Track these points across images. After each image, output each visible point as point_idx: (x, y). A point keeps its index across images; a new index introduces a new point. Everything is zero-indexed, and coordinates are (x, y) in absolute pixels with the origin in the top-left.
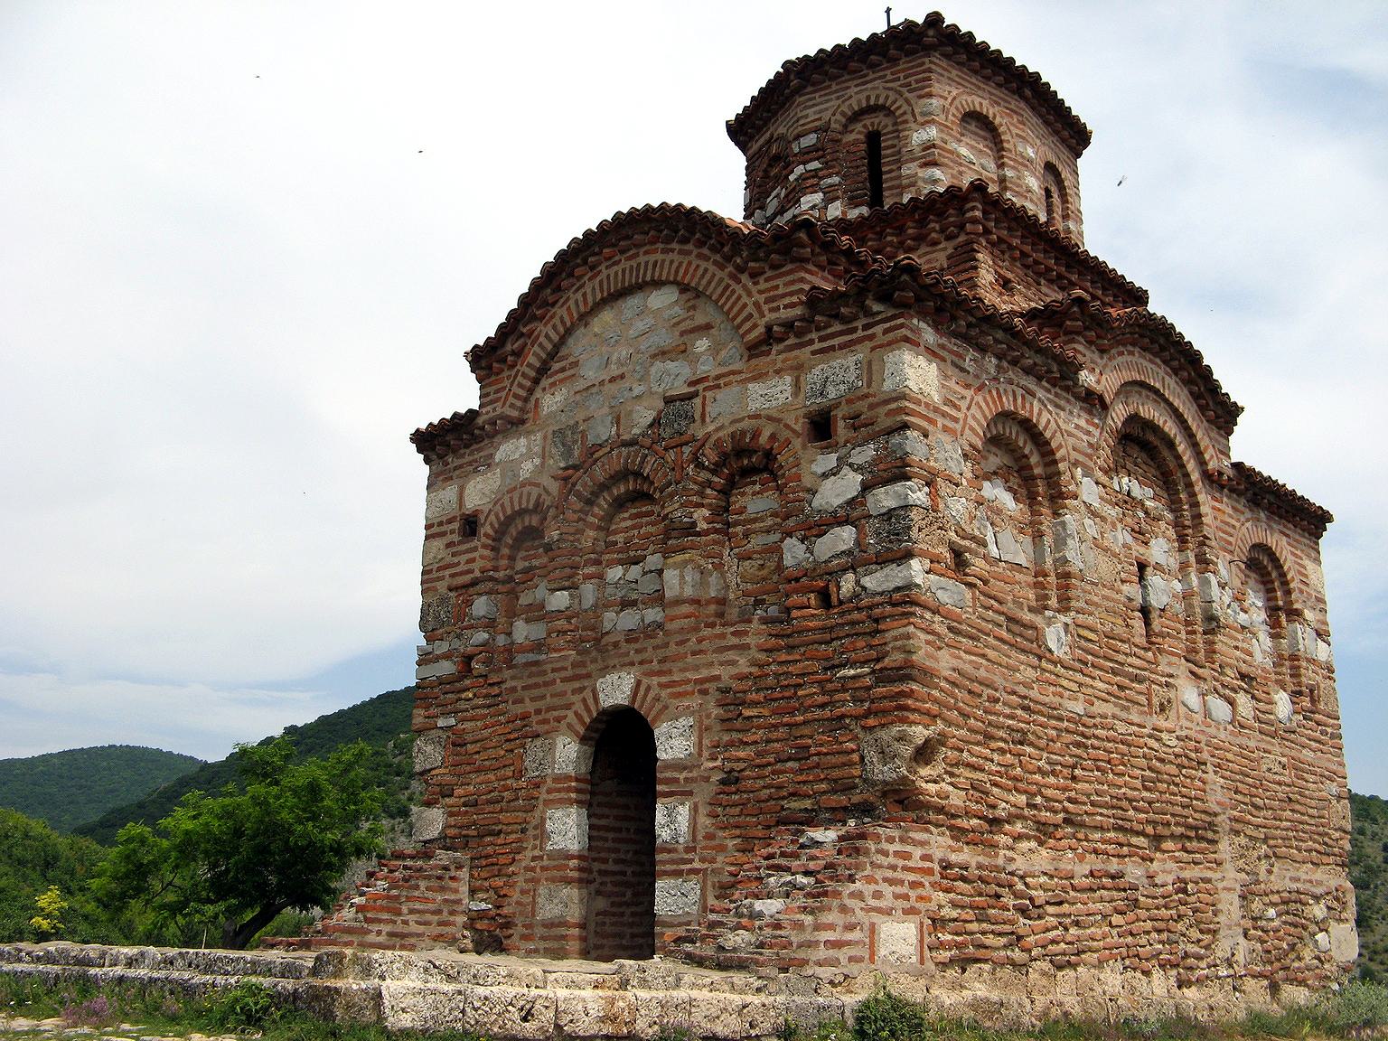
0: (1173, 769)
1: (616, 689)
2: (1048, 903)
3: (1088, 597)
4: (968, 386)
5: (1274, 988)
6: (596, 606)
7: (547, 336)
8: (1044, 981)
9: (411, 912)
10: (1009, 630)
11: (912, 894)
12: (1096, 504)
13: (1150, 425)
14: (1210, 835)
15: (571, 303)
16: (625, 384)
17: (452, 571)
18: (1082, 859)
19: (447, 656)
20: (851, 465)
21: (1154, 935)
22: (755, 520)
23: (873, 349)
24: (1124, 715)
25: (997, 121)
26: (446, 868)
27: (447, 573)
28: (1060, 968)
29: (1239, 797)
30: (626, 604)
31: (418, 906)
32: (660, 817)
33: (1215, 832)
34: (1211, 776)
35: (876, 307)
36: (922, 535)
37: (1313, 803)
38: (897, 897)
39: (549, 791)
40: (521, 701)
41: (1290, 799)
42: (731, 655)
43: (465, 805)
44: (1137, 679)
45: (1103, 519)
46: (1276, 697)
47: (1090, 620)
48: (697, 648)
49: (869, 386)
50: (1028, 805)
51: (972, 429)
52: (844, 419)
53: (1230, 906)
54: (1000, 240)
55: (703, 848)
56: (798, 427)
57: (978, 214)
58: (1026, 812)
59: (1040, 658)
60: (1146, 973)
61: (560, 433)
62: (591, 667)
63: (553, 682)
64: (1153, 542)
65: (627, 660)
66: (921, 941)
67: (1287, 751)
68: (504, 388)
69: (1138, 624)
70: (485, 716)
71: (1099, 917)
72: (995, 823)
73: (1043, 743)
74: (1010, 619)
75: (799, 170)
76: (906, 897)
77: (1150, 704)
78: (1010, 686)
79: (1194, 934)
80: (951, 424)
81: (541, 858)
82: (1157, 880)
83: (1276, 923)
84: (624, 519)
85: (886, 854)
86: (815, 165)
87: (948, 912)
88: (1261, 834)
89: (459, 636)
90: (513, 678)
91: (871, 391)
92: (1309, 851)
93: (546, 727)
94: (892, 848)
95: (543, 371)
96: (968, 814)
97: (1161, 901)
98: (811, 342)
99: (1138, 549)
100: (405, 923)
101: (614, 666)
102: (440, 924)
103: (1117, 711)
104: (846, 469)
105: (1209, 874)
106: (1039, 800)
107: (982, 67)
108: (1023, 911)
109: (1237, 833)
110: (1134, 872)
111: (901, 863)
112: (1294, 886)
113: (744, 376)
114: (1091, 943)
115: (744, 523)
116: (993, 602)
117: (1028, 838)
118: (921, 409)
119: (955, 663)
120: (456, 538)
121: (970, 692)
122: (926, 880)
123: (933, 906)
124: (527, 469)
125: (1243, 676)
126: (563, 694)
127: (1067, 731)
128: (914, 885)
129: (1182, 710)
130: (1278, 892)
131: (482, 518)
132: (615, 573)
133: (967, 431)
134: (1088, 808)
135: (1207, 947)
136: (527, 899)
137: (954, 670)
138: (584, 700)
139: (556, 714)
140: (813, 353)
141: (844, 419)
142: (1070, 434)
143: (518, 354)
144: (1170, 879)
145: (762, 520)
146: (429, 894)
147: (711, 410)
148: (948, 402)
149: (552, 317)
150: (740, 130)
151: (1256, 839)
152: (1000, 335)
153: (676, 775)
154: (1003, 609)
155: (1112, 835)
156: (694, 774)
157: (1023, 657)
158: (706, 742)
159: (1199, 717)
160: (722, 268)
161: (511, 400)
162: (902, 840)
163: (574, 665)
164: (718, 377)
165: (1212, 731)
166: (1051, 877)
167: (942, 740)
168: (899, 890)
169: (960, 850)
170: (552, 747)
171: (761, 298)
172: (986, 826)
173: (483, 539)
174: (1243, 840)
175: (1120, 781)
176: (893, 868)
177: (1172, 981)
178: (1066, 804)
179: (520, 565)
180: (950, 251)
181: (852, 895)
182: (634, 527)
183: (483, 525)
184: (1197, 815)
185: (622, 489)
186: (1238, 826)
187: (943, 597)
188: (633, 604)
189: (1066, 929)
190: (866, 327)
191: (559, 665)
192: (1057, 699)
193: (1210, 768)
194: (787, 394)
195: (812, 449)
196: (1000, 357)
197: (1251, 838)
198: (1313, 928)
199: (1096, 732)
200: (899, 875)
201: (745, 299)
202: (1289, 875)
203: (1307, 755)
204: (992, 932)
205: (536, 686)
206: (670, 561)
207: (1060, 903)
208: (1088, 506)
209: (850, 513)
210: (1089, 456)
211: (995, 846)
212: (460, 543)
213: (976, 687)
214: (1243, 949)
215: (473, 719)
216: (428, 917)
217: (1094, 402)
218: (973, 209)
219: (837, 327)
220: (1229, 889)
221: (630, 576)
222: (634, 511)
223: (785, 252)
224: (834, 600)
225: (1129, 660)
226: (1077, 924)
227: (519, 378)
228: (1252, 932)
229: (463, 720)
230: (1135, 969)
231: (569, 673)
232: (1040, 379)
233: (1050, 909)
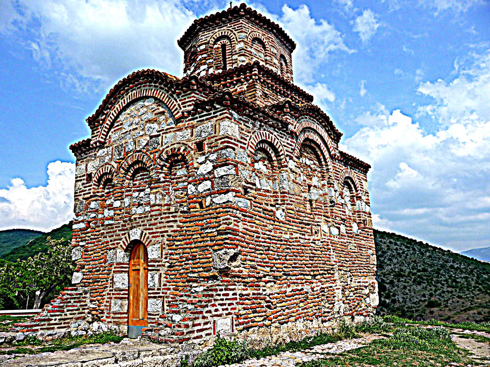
0: (319, 252)
1: (135, 234)
2: (277, 303)
4: (249, 132)
6: (129, 205)
7: (113, 114)
8: (277, 330)
9: (68, 311)
10: (264, 213)
11: (229, 308)
12: (294, 168)
13: (312, 141)
14: (332, 272)
15: (120, 103)
16: (137, 131)
17: (84, 193)
18: (289, 286)
19: (82, 221)
20: (209, 160)
21: (314, 308)
22: (179, 178)
24: (303, 237)
25: (264, 41)
26: (81, 294)
27: (82, 193)
28: (282, 324)
29: (341, 258)
30: (140, 205)
31: (70, 308)
34: (332, 253)
35: (217, 106)
36: (233, 184)
37: (365, 257)
38: (223, 310)
39: (115, 268)
42: (171, 224)
43: (88, 272)
44: (308, 224)
45: (296, 173)
46: (352, 225)
48: (161, 221)
49: (215, 133)
50: (271, 271)
51: (251, 147)
52: (207, 144)
53: (339, 293)
54: (264, 81)
55: (163, 289)
56: (193, 147)
57: (257, 72)
59: (274, 221)
60: (312, 321)
63: (116, 231)
64: (313, 178)
66: (233, 324)
67: (356, 242)
68: (99, 132)
69: (308, 205)
71: (295, 305)
73: (275, 249)
75: (200, 57)
76: (227, 309)
77: (312, 232)
79: (327, 305)
80: (244, 146)
82: (315, 289)
83: (354, 297)
84: (139, 176)
85: (219, 295)
86: (205, 55)
88: (348, 269)
89: (86, 215)
90: (103, 229)
91: (216, 135)
92: (363, 272)
93: (114, 246)
94: (221, 293)
95: (111, 126)
96: (250, 276)
97: (316, 296)
98: (197, 118)
99: (308, 181)
100: (66, 315)
102: (79, 314)
103: (301, 236)
104: (208, 162)
105: (331, 285)
106: (274, 269)
107: (260, 22)
108: (269, 307)
109: (341, 270)
110: (307, 288)
111: (225, 297)
112: (359, 284)
113: (175, 129)
114: (292, 314)
115: (176, 178)
116: (258, 204)
117: (270, 281)
118: (233, 141)
120: (85, 182)
121: (250, 235)
122: (234, 302)
123: (237, 311)
125: (342, 219)
126: (119, 235)
127: (284, 244)
128: (229, 305)
129: (323, 232)
131: (93, 175)
133: (249, 147)
135: (331, 309)
136: (108, 304)
137: (244, 229)
138: (126, 238)
139: (117, 242)
140: (197, 122)
141: (207, 144)
142: (285, 146)
143: (104, 120)
144: (319, 288)
145: (182, 178)
146: (75, 304)
147: (165, 141)
148: (242, 138)
149: (114, 108)
150: (182, 43)
151: (346, 271)
152: (261, 114)
153: (154, 264)
156: (160, 263)
157: (268, 222)
158: (164, 253)
159: (328, 234)
160: (168, 92)
161: (101, 136)
163: (122, 226)
164: (167, 129)
165: (332, 238)
166: (279, 294)
167: (240, 253)
168: (224, 307)
169: (247, 289)
171: (180, 103)
172: (256, 280)
173: (94, 182)
174: (342, 272)
175: (302, 258)
176: (222, 300)
177: (320, 322)
178: (284, 269)
179: (106, 191)
180: (247, 85)
181: (207, 312)
182: (141, 179)
184: (328, 266)
185: (137, 166)
186: (341, 268)
187: (240, 204)
189: (284, 311)
190: (214, 113)
191: (117, 225)
192: (280, 234)
193: (332, 250)
194: (189, 136)
196: (261, 121)
197: (345, 271)
198: (365, 296)
199: (294, 244)
200: (224, 302)
201: (175, 103)
202: (357, 281)
203: (363, 242)
204: (258, 316)
205: (110, 232)
206: (152, 191)
208: (291, 169)
209: (210, 176)
210: (291, 153)
211: (259, 286)
212: (86, 183)
213: (252, 234)
215: (91, 243)
216: (74, 312)
218: (255, 70)
219: (205, 113)
220: (338, 289)
221: (140, 196)
222: (141, 174)
223: (188, 87)
224: (204, 206)
225: (305, 218)
226: (288, 308)
227: (104, 128)
228: (346, 301)
229: (87, 244)
230: (307, 320)
231: (121, 228)
232: (275, 128)
233: (278, 305)
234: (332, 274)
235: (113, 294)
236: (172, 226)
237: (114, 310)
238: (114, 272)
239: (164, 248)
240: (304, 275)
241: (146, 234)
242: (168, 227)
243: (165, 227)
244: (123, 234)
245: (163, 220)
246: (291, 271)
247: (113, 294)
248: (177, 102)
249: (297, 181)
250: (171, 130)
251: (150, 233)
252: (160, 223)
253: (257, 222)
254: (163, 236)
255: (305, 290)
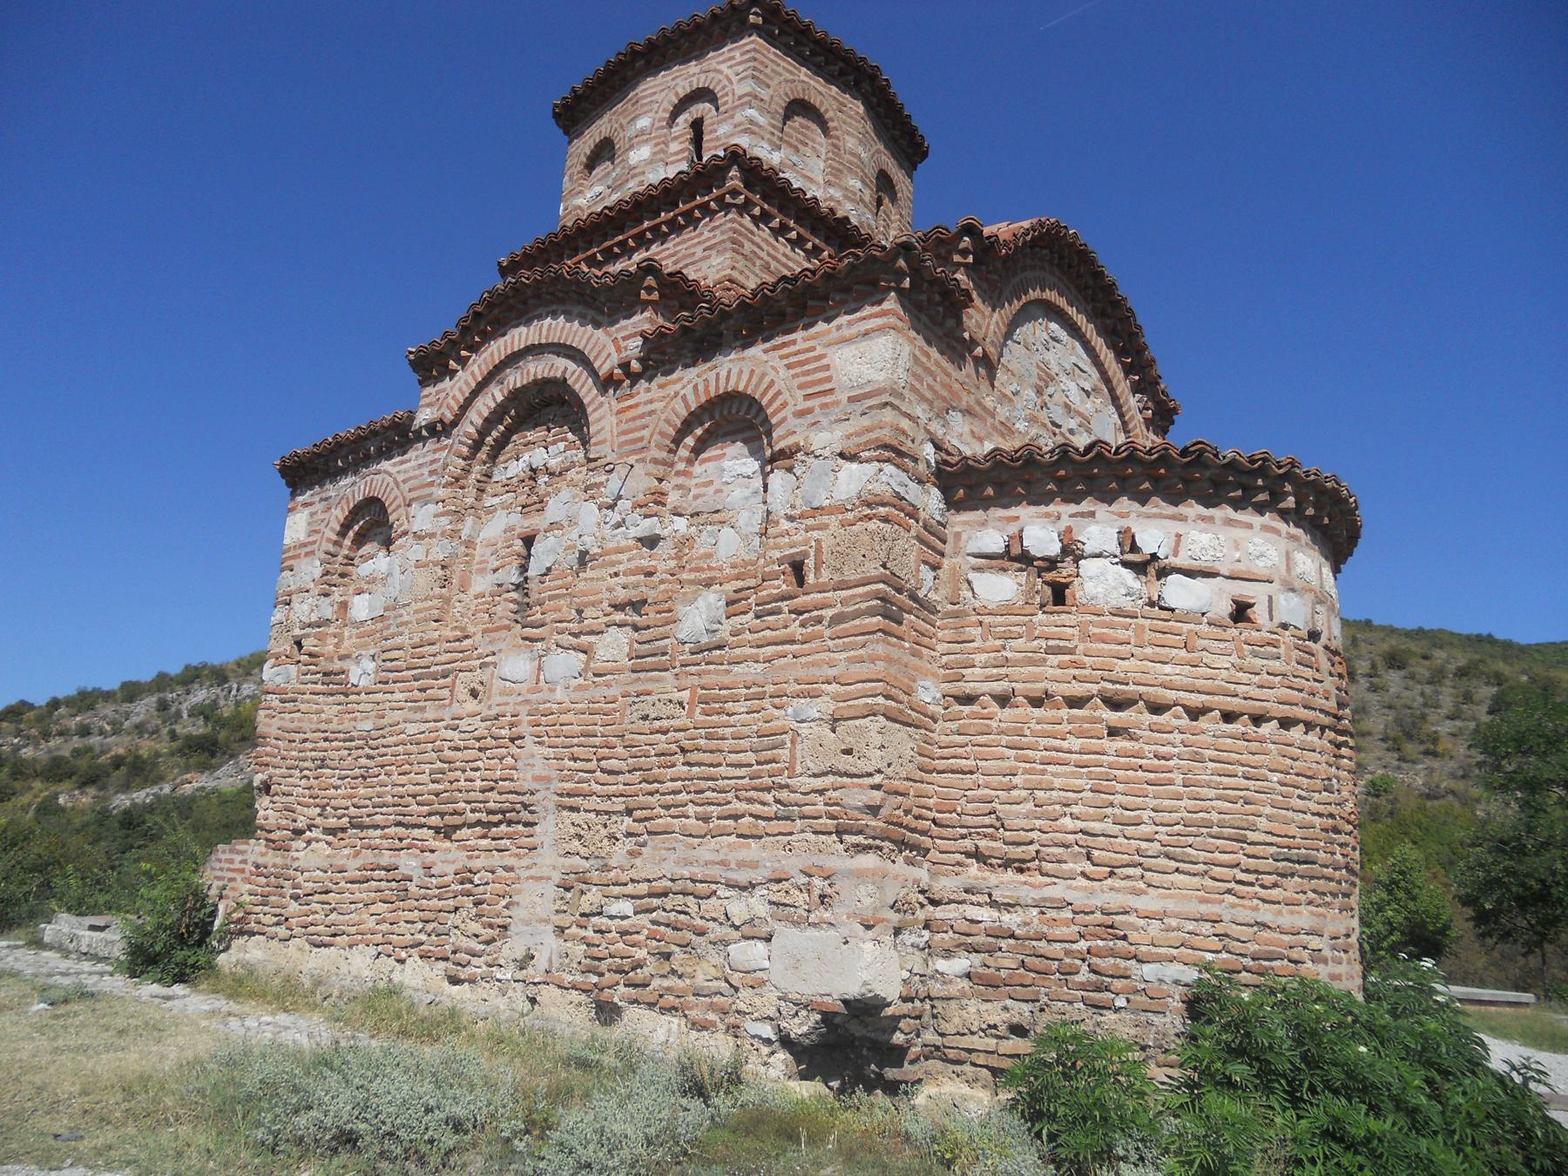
3: (399, 620)
5: (607, 1012)
14: (525, 816)
18: (357, 854)
33: (532, 812)
41: (683, 750)
45: (432, 535)
47: (398, 640)
58: (318, 820)
59: (346, 695)
71: (361, 905)
72: (298, 833)
74: (325, 674)
78: (314, 727)
82: (433, 871)
85: (220, 861)
87: (247, 898)
103: (411, 715)
108: (296, 898)
110: (409, 863)
118: (291, 554)
119: (280, 723)
122: (239, 877)
125: (618, 607)
130: (649, 881)
134: (370, 810)
144: (450, 869)
154: (318, 669)
155: (391, 831)
162: (231, 851)
176: (221, 869)
207: (327, 892)
214: (548, 948)
217: (439, 430)
225: (439, 658)
233: (317, 897)
234: (527, 824)
240: (406, 826)
246: (369, 816)
249: (430, 558)
253: (303, 707)
255: (403, 870)
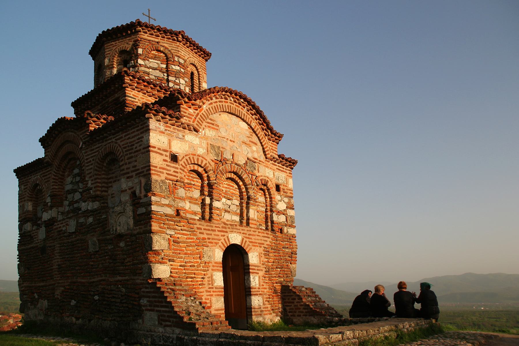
1: (236, 239)
22: (260, 203)
23: (287, 176)
32: (252, 279)
40: (203, 233)
42: (266, 239)
43: (180, 266)
48: (258, 234)
55: (262, 288)
61: (213, 146)
62: (228, 230)
63: (215, 231)
65: (239, 231)
70: (188, 235)
81: (213, 288)
91: (287, 186)
93: (212, 244)
98: (276, 165)
101: (235, 232)
124: (201, 151)
126: (218, 235)
132: (224, 200)
139: (215, 241)
140: (277, 168)
153: (254, 268)
156: (259, 268)
160: (262, 132)
163: (222, 227)
164: (260, 161)
170: (213, 251)
183: (181, 160)
188: (229, 212)
191: (217, 226)
195: (276, 193)
205: (209, 230)
231: (221, 229)
235: (213, 292)
236: (266, 241)
237: (217, 307)
238: (212, 270)
239: (262, 256)
241: (246, 241)
242: (264, 240)
243: (262, 240)
244: (222, 236)
245: (260, 234)
247: (213, 292)
248: (268, 144)
250: (262, 163)
251: (250, 242)
252: (257, 235)
254: (261, 247)
